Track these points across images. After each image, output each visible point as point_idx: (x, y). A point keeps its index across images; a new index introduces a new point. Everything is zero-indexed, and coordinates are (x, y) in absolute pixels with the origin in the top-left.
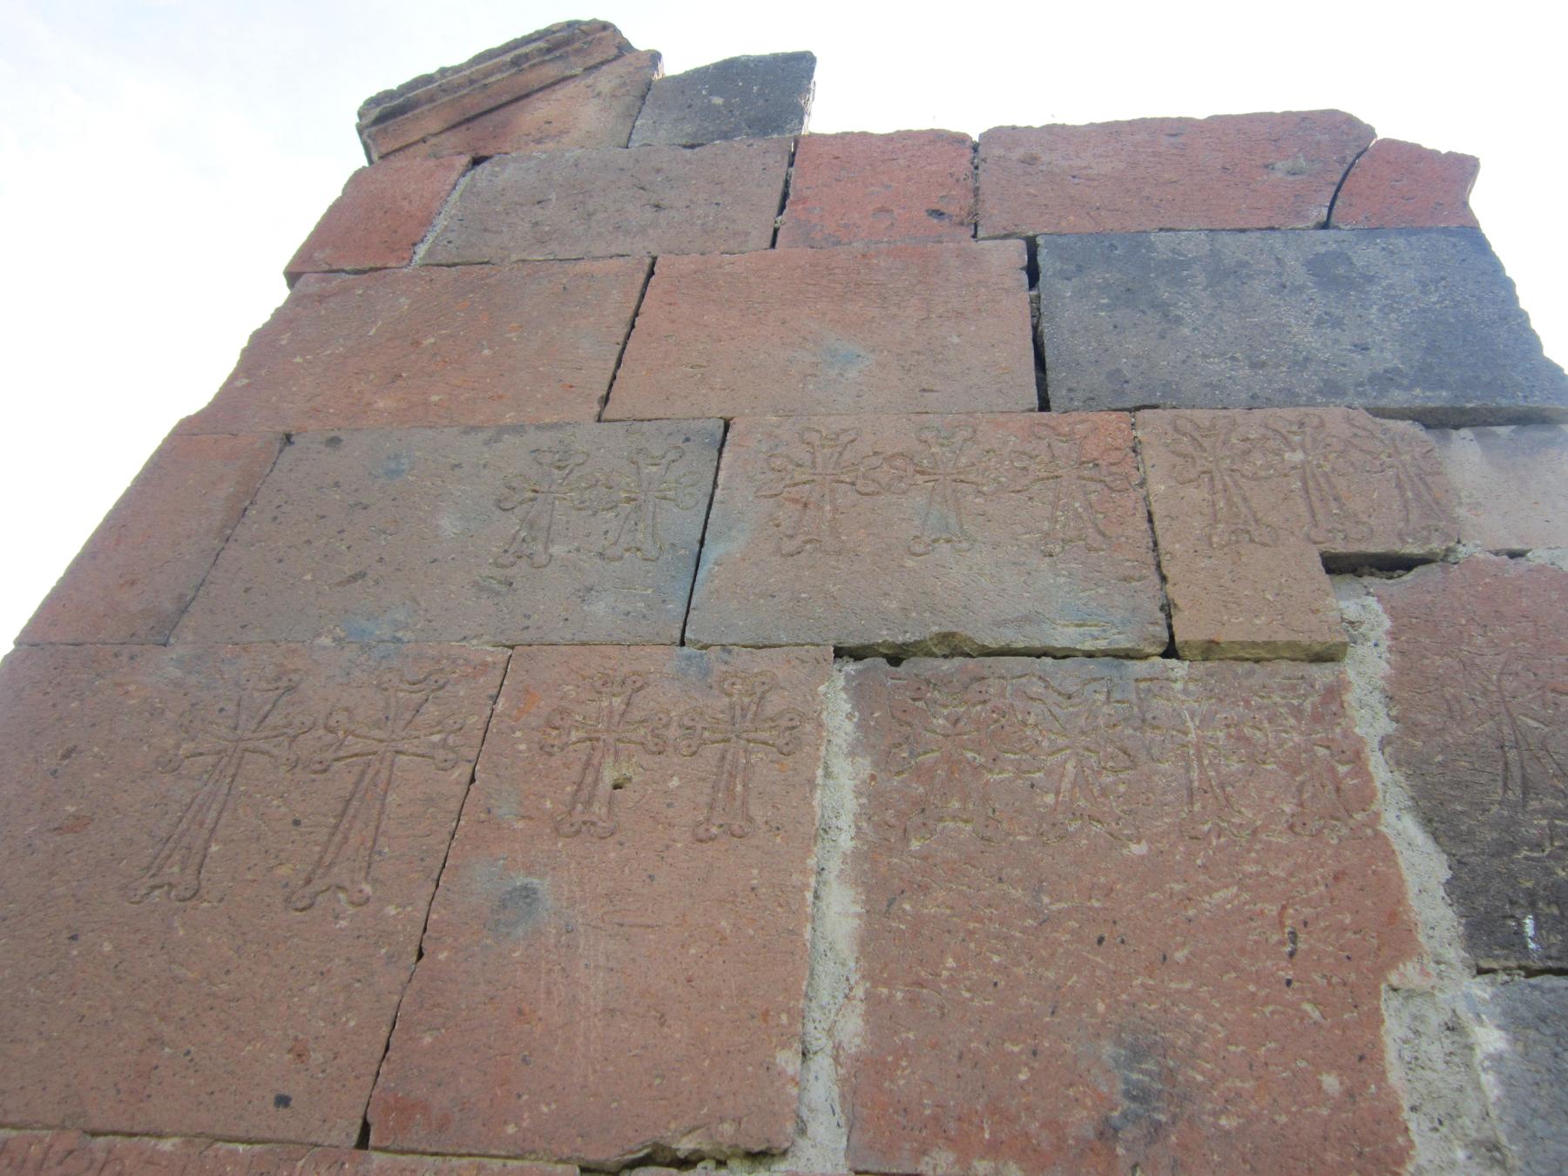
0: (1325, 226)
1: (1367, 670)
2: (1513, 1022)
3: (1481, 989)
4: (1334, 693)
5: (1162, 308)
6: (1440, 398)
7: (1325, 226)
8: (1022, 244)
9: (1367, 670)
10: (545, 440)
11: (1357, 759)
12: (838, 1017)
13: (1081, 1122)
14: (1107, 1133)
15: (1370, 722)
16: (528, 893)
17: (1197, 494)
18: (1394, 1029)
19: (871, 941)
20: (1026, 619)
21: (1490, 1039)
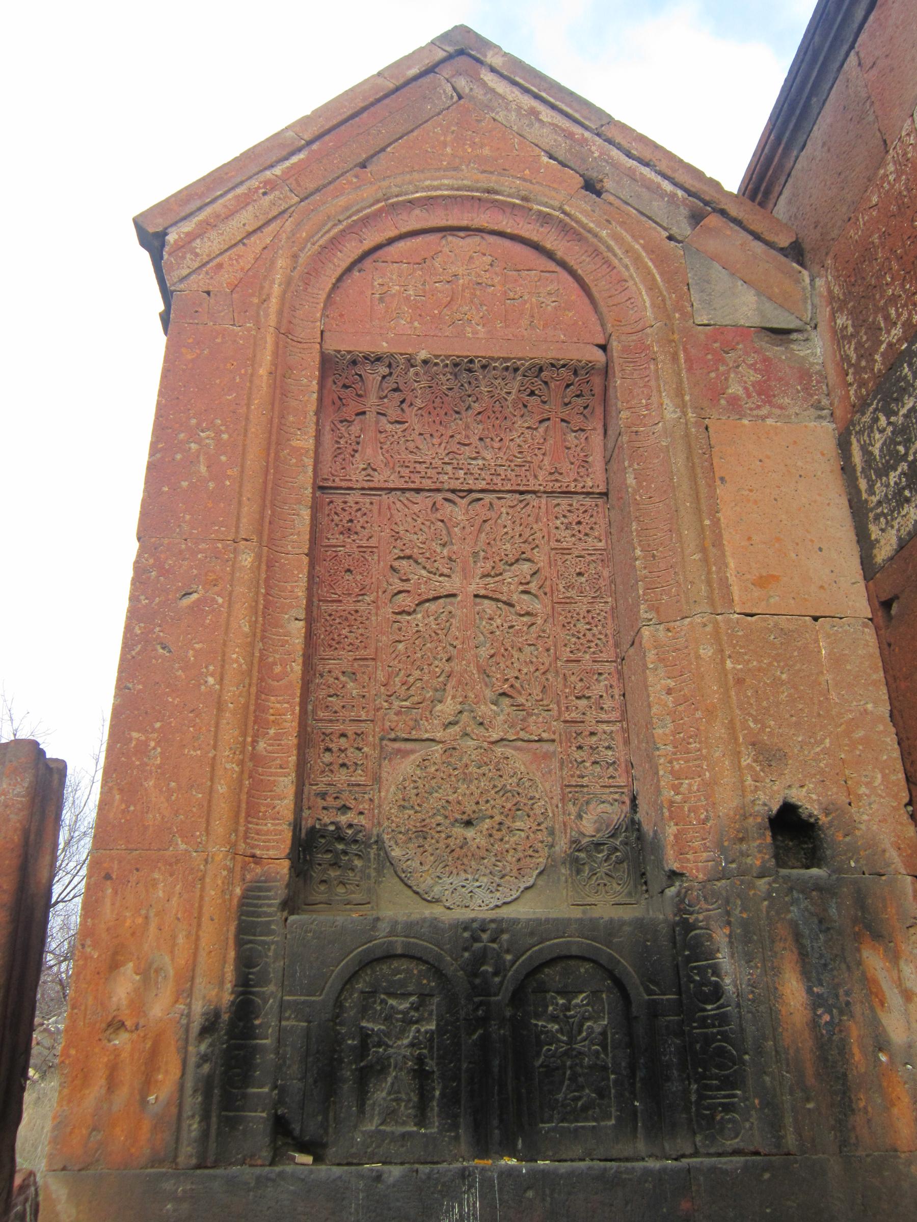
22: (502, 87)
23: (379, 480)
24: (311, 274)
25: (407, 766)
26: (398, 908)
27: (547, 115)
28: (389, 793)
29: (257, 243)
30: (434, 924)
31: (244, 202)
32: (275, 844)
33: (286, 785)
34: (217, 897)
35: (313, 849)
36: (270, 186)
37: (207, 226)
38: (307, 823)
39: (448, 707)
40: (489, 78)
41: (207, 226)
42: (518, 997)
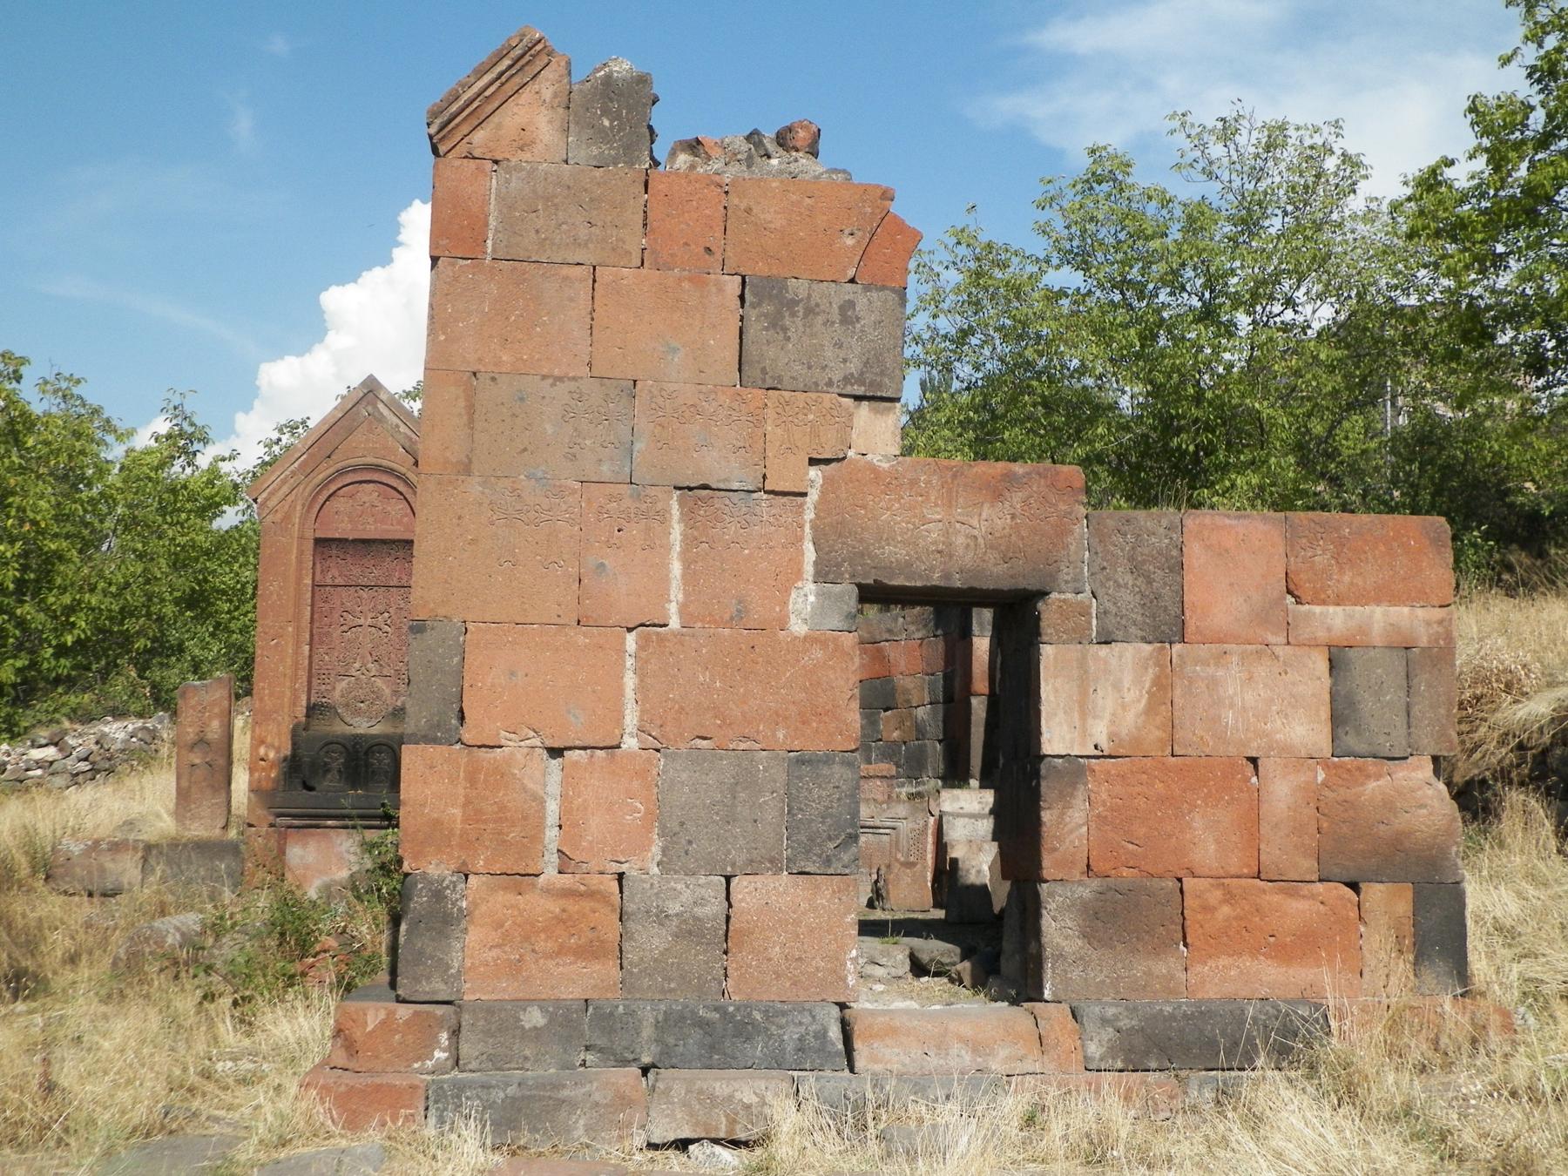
0: (852, 281)
1: (814, 496)
2: (817, 595)
3: (812, 586)
4: (802, 505)
5: (785, 329)
6: (860, 391)
7: (852, 281)
8: (739, 278)
9: (814, 496)
10: (572, 385)
11: (801, 527)
12: (676, 593)
13: (727, 617)
14: (732, 618)
15: (809, 515)
16: (602, 565)
17: (779, 431)
18: (793, 595)
19: (684, 576)
20: (726, 480)
21: (812, 598)
22: (385, 412)
23: (337, 582)
24: (310, 507)
25: (344, 684)
26: (339, 728)
27: (403, 428)
28: (337, 693)
29: (290, 498)
30: (344, 736)
31: (284, 482)
32: (301, 712)
33: (304, 697)
34: (287, 726)
35: (311, 710)
36: (293, 474)
37: (272, 494)
38: (313, 700)
39: (357, 665)
40: (380, 406)
41: (272, 494)
42: (366, 753)
